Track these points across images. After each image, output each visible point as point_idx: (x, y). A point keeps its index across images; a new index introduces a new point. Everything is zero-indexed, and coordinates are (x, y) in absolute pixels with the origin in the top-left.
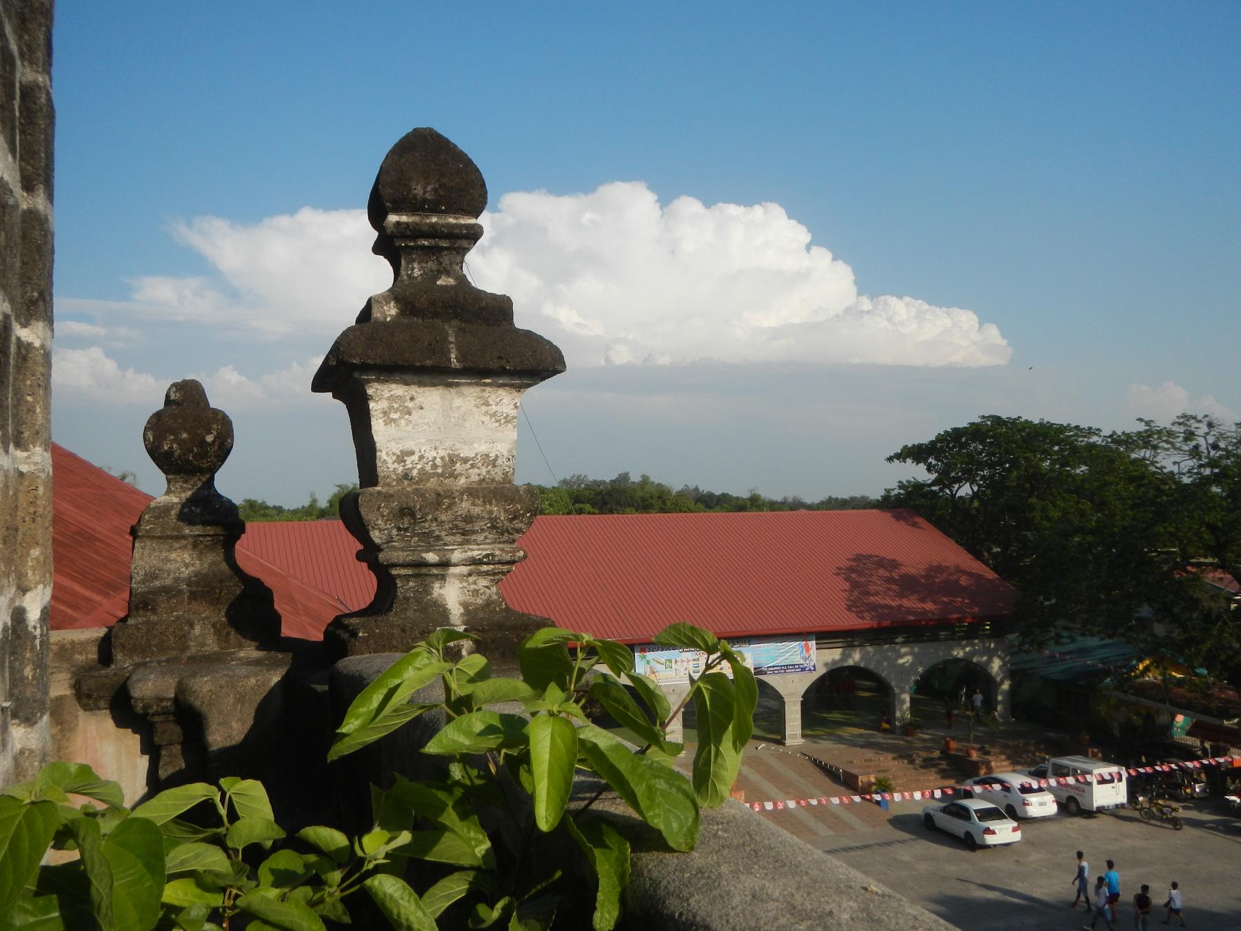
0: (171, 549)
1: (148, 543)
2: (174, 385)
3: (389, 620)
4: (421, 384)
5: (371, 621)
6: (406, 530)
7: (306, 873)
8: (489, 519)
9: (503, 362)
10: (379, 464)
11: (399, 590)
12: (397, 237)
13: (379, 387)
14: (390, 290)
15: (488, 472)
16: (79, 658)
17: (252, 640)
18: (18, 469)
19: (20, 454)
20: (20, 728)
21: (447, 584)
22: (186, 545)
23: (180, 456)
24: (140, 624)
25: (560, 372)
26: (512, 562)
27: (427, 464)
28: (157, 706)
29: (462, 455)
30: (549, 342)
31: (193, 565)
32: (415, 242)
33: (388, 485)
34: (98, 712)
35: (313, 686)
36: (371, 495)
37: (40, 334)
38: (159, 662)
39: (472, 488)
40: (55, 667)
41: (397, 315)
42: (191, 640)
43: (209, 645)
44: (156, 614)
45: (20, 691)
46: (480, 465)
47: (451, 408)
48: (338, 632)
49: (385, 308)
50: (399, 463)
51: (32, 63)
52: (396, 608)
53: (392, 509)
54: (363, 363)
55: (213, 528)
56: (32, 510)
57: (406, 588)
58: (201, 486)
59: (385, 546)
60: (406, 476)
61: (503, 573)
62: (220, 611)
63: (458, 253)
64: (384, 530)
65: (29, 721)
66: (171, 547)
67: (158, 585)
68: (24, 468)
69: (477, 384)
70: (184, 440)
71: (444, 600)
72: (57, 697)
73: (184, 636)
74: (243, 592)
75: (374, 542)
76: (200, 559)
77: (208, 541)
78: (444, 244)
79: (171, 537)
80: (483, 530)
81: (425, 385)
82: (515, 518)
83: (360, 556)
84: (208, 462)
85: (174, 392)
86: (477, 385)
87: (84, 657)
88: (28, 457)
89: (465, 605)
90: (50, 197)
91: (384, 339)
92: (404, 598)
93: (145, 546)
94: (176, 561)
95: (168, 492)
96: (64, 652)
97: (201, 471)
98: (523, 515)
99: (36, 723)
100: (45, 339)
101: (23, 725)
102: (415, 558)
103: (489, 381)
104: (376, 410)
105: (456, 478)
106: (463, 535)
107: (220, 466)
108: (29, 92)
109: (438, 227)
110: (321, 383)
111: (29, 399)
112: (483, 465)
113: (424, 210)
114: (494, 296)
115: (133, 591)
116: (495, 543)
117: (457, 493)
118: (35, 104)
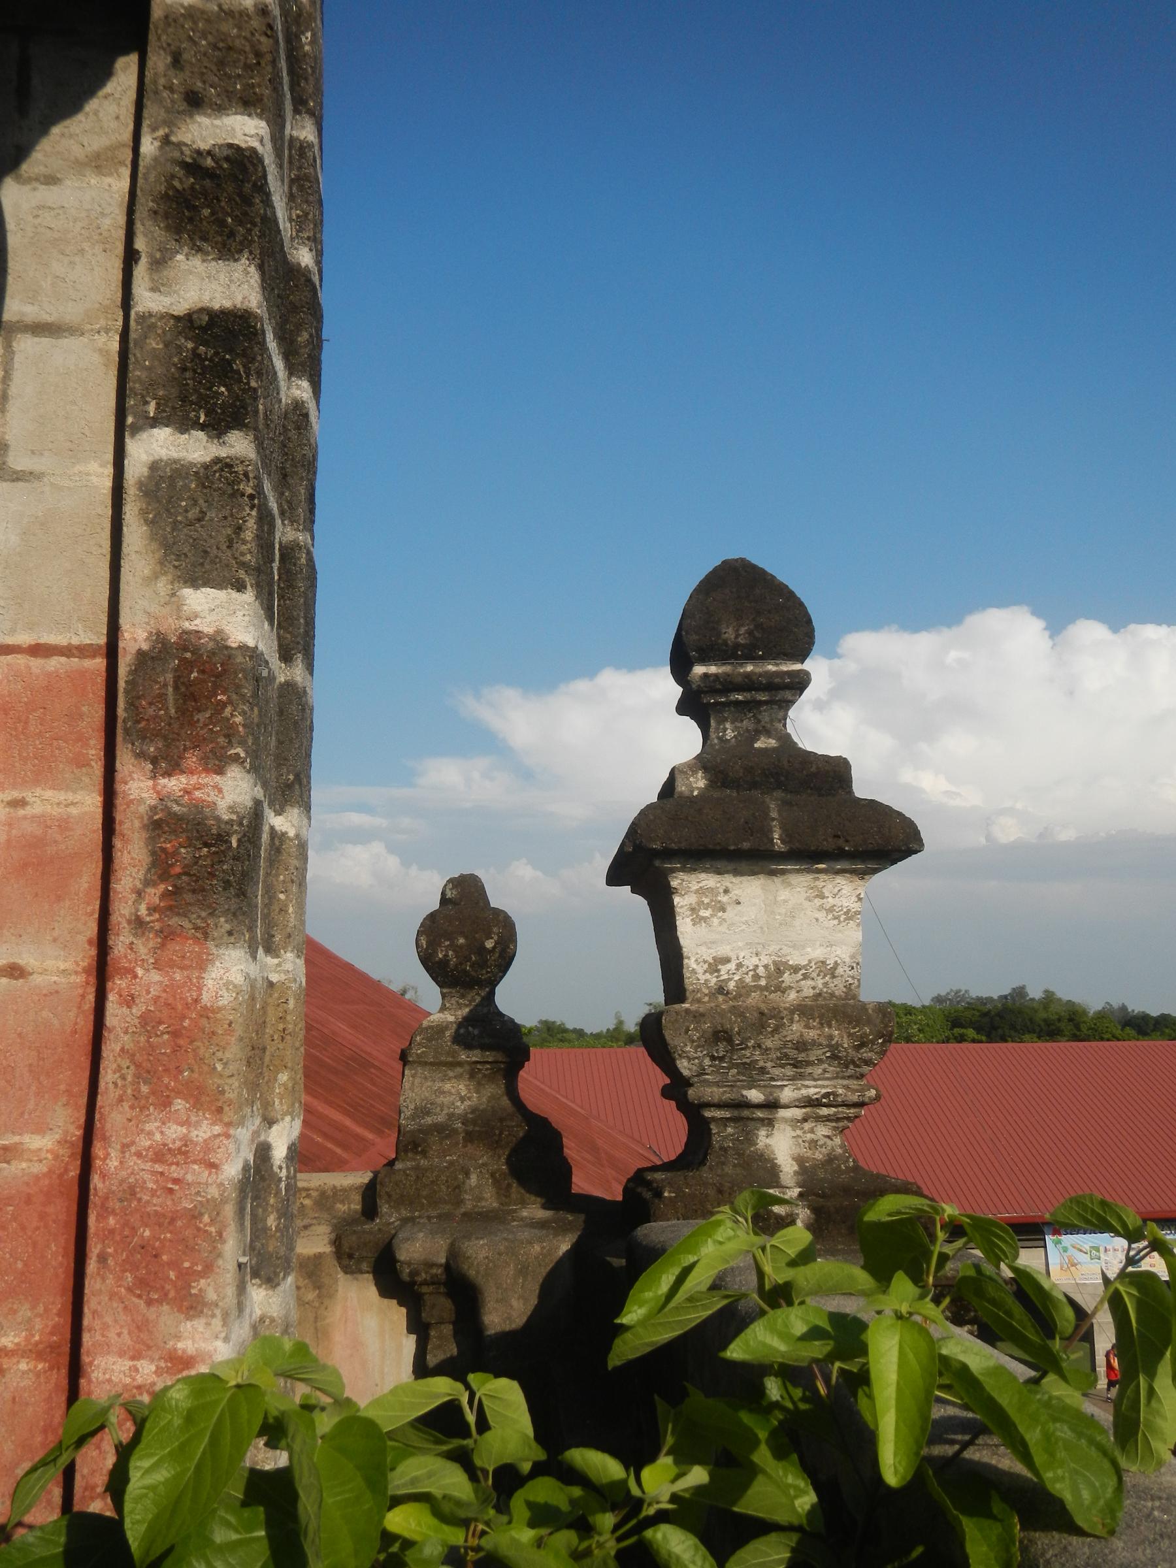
1: (420, 1070)
2: (450, 881)
4: (737, 873)
5: (678, 1177)
6: (721, 1059)
7: (570, 1512)
8: (829, 1046)
9: (841, 842)
10: (687, 974)
11: (714, 1138)
12: (705, 693)
13: (685, 878)
14: (698, 757)
15: (826, 984)
16: (342, 1208)
17: (538, 1194)
18: (267, 978)
19: (271, 961)
20: (261, 1290)
21: (775, 1132)
22: (462, 1074)
23: (456, 965)
24: (409, 1169)
25: (916, 852)
26: (861, 1105)
27: (747, 974)
28: (426, 1273)
29: (791, 963)
30: (899, 814)
31: (469, 1098)
32: (727, 696)
33: (699, 1001)
34: (360, 1276)
35: (608, 1259)
36: (677, 1013)
37: (295, 823)
38: (429, 1218)
39: (806, 1006)
40: (315, 1218)
41: (707, 787)
43: (487, 1200)
44: (425, 1157)
45: (262, 1245)
46: (814, 975)
47: (776, 902)
48: (639, 1190)
49: (691, 779)
50: (711, 974)
51: (292, 522)
52: (711, 1160)
53: (704, 1032)
55: (494, 1053)
56: (281, 1027)
57: (723, 1135)
59: (696, 1079)
60: (721, 990)
61: (848, 1118)
62: (499, 1157)
63: (780, 708)
65: (271, 1282)
66: (445, 1076)
68: (274, 978)
69: (809, 871)
70: (461, 947)
71: (773, 1152)
73: (458, 1187)
75: (681, 1074)
77: (487, 1069)
78: (763, 697)
79: (445, 1064)
80: (820, 1061)
81: (742, 874)
82: (862, 1045)
83: (667, 1093)
84: (488, 972)
85: (451, 889)
86: (808, 873)
87: (346, 1207)
88: (279, 965)
89: (799, 1160)
90: (310, 667)
92: (721, 1148)
93: (416, 1074)
94: (451, 1093)
95: (443, 1009)
96: (325, 1199)
97: (480, 983)
98: (873, 1042)
99: (278, 1284)
100: (301, 827)
101: (264, 1286)
102: (733, 1096)
103: (823, 866)
104: (682, 907)
105: (783, 992)
106: (795, 1066)
107: (502, 978)
108: (289, 553)
109: (754, 678)
110: (615, 877)
111: (282, 896)
112: (818, 975)
113: (737, 658)
114: (827, 759)
115: (402, 1128)
116: (836, 1078)
117: (785, 1012)
118: (295, 565)
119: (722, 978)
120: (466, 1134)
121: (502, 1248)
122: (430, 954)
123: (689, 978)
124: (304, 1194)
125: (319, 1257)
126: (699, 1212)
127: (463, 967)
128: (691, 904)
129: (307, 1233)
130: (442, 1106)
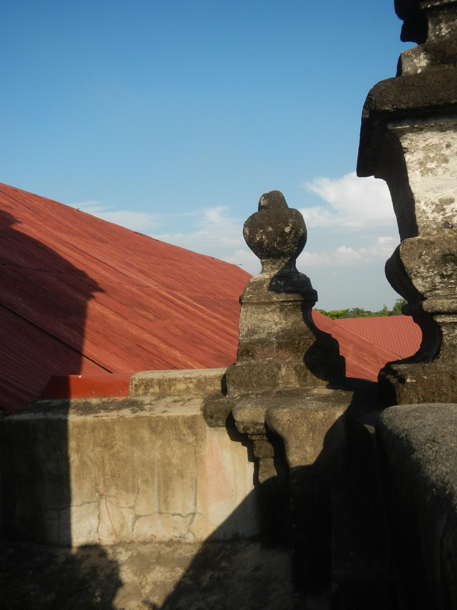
0: (265, 312)
1: (250, 308)
2: (264, 195)
3: (436, 367)
5: (417, 367)
6: (450, 277)
10: (418, 214)
11: (444, 338)
13: (414, 138)
16: (210, 389)
17: (325, 379)
23: (268, 244)
24: (244, 366)
28: (253, 428)
31: (280, 323)
33: (429, 234)
35: (366, 426)
38: (257, 394)
40: (196, 394)
41: (428, 66)
42: (279, 378)
43: (292, 383)
44: (254, 359)
48: (388, 377)
49: (415, 61)
50: (438, 212)
52: (443, 354)
53: (434, 256)
54: (397, 110)
55: (294, 295)
58: (285, 266)
59: (428, 294)
62: (299, 357)
64: (427, 278)
67: (257, 338)
70: (270, 233)
72: (192, 416)
73: (274, 376)
74: (316, 343)
75: (416, 290)
76: (285, 319)
77: (290, 306)
85: (263, 200)
87: (213, 388)
91: (416, 84)
92: (451, 345)
94: (269, 321)
95: (263, 271)
104: (412, 162)
115: (240, 342)
119: (447, 215)
120: (278, 344)
121: (298, 414)
122: (252, 239)
123: (420, 217)
124: (189, 381)
125: (194, 417)
126: (436, 394)
127: (272, 245)
128: (419, 159)
129: (189, 403)
130: (264, 329)
